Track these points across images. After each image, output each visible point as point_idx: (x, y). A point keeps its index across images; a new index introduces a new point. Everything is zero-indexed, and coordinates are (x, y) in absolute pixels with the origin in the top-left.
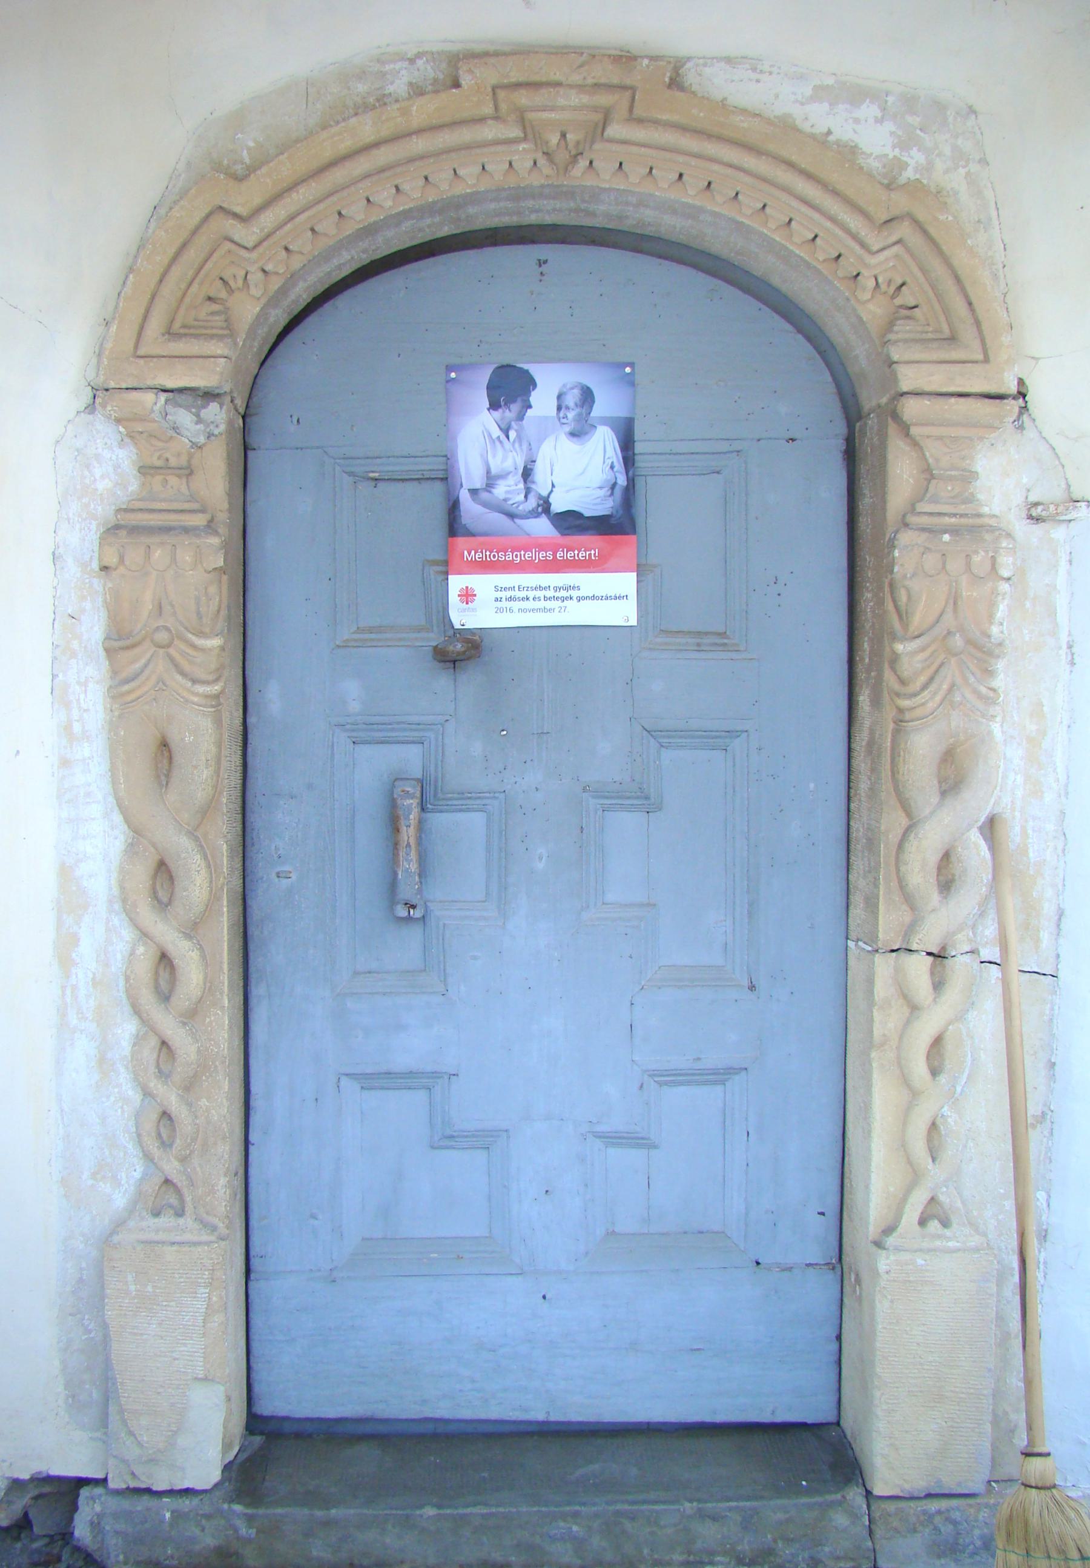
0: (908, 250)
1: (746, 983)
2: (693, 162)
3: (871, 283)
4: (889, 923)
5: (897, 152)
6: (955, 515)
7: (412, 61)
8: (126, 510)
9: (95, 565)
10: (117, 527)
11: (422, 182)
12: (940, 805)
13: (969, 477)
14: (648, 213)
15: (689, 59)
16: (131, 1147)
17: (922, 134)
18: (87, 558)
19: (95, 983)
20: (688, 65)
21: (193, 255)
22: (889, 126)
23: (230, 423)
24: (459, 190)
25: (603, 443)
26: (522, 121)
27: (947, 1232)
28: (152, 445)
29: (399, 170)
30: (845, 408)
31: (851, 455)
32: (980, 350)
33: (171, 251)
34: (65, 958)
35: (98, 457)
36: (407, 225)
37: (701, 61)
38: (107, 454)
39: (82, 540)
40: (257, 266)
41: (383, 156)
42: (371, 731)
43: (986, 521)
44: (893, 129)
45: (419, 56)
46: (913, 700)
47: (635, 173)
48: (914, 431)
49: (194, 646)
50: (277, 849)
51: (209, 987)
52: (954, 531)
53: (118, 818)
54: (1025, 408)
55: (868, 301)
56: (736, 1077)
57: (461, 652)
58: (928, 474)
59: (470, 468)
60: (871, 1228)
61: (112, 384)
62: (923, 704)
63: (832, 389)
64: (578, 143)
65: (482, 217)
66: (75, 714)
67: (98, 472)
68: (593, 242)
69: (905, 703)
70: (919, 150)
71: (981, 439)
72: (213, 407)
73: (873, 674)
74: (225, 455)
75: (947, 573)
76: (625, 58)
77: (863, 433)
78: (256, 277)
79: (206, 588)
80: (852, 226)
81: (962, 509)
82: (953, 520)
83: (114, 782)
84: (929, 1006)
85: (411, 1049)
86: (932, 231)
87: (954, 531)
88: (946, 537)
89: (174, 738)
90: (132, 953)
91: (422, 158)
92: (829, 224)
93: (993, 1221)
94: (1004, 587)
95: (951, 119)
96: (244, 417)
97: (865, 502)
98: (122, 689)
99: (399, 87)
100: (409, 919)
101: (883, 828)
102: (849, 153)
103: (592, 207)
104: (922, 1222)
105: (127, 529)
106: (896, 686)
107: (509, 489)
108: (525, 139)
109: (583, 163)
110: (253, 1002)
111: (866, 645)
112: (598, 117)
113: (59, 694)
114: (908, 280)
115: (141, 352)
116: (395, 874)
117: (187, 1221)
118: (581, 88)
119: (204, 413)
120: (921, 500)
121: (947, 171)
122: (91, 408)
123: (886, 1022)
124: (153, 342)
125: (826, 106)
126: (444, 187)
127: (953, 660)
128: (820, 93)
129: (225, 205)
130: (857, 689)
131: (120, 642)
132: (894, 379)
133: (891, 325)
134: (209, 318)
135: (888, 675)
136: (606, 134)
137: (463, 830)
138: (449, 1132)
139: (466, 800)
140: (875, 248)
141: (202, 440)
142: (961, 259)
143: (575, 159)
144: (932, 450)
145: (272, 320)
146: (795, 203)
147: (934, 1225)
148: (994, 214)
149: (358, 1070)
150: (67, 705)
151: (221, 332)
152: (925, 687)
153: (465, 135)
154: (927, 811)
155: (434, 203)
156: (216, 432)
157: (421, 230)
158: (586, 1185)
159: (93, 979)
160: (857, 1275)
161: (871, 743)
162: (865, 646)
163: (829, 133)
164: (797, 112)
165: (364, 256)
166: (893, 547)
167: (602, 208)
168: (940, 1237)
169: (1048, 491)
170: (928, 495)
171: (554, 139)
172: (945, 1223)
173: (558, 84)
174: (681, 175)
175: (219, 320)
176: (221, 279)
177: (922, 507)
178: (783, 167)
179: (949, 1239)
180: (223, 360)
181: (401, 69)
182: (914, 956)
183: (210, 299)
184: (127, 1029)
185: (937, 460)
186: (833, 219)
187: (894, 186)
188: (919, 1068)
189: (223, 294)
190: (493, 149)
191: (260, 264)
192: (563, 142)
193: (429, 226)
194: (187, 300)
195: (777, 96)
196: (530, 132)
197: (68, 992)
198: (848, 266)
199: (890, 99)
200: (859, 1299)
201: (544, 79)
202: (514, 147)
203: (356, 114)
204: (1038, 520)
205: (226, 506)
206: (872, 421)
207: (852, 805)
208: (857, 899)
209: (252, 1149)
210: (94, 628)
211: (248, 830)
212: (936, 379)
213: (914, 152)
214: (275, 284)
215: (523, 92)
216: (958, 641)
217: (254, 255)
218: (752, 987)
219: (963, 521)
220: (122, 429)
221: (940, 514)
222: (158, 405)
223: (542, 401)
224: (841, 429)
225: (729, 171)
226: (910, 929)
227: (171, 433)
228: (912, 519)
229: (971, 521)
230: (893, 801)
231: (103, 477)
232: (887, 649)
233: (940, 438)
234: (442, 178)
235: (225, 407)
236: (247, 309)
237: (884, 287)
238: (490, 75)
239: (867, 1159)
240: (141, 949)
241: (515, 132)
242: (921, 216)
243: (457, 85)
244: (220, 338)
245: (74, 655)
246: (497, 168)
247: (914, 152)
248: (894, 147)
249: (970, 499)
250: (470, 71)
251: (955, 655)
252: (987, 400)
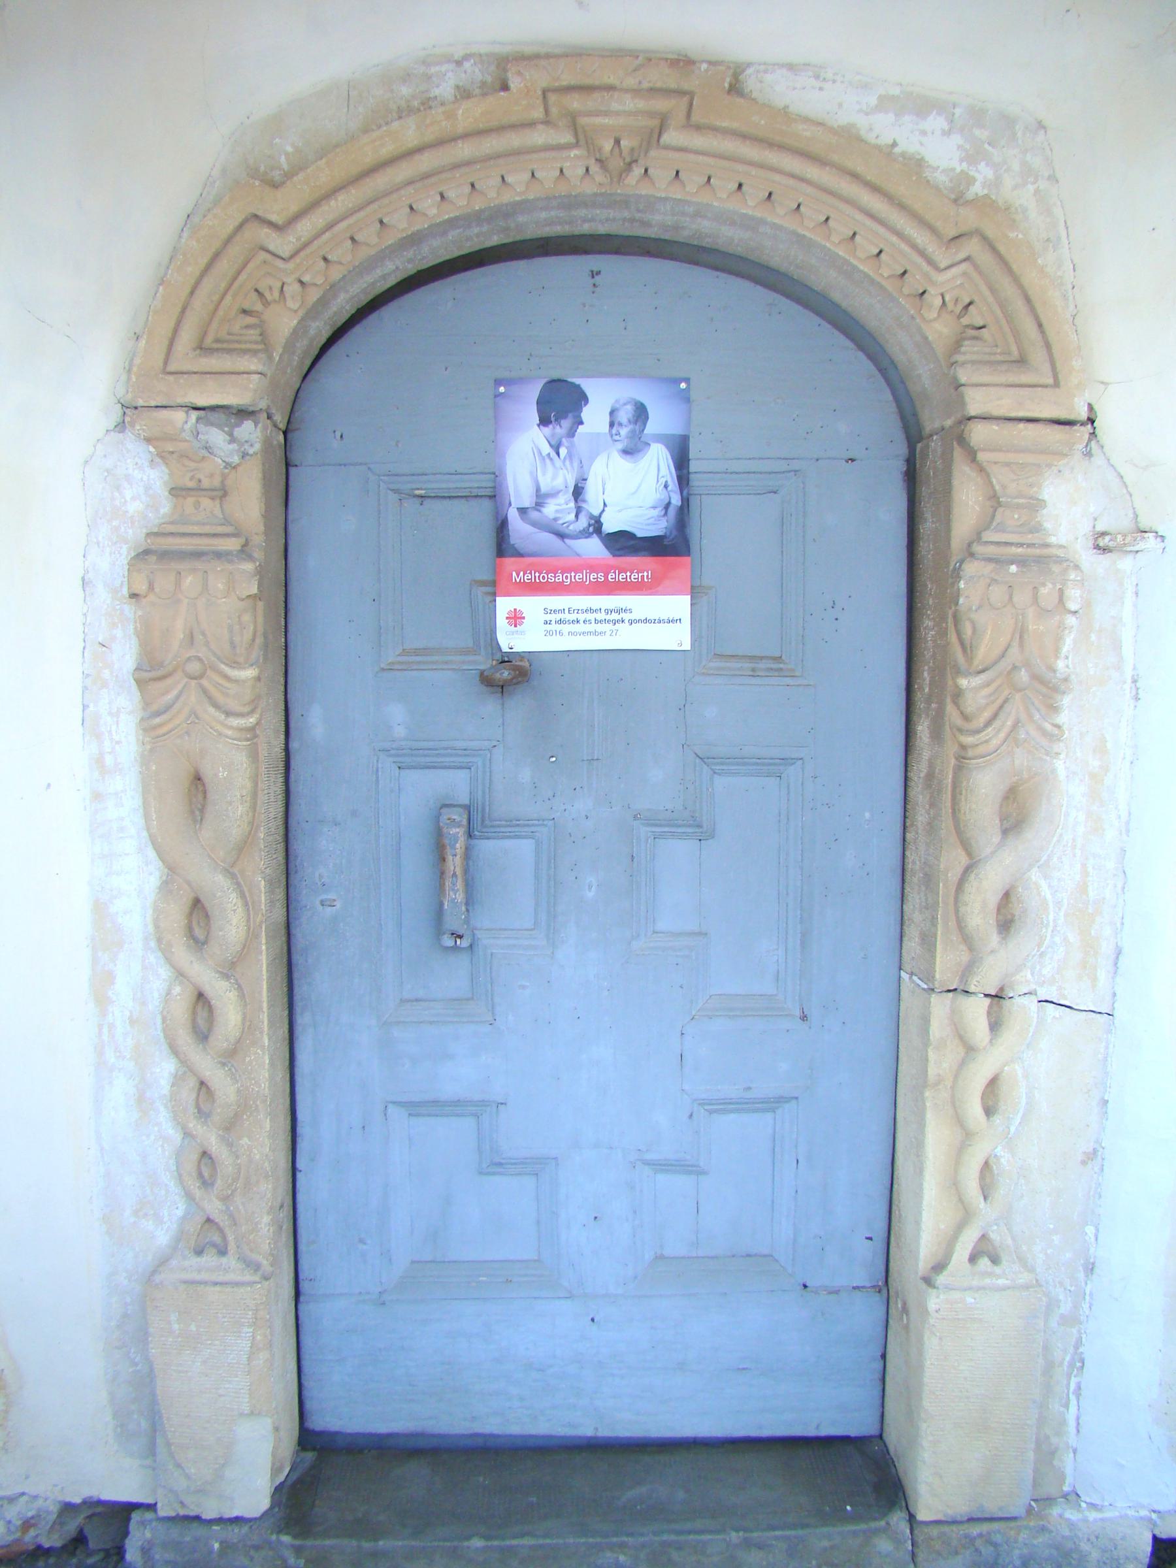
0: (976, 267)
1: (798, 1013)
2: (754, 171)
3: (939, 301)
4: (947, 962)
5: (964, 165)
6: (1021, 545)
7: (459, 63)
8: (156, 534)
9: (125, 591)
10: (147, 552)
11: (468, 189)
12: (1000, 845)
13: (1036, 505)
14: (706, 223)
15: (749, 65)
16: (173, 1185)
17: (990, 149)
18: (118, 583)
19: (132, 1021)
20: (749, 71)
21: (225, 266)
22: (957, 139)
23: (267, 443)
24: (507, 197)
25: (657, 462)
26: (574, 127)
27: (997, 1270)
28: (184, 465)
29: (444, 176)
30: (906, 428)
31: (911, 477)
32: (1050, 374)
33: (204, 261)
34: (101, 998)
35: (128, 478)
36: (453, 234)
37: (762, 67)
38: (137, 474)
39: (112, 563)
40: (294, 276)
41: (426, 162)
42: (415, 757)
43: (1054, 551)
44: (961, 142)
45: (467, 57)
46: (977, 737)
47: (693, 181)
48: (981, 456)
49: (227, 677)
50: (321, 876)
51: (248, 1027)
52: (1022, 562)
53: (151, 854)
54: (1093, 434)
55: (935, 319)
56: (787, 1106)
57: (510, 676)
58: (994, 500)
59: (519, 485)
60: (921, 1265)
61: (141, 403)
62: (986, 742)
63: (893, 408)
64: (632, 149)
65: (532, 226)
66: (107, 745)
67: (128, 494)
68: (648, 254)
69: (968, 740)
70: (987, 165)
71: (1049, 466)
72: (248, 425)
73: (933, 705)
74: (260, 475)
75: (1014, 606)
76: (683, 62)
77: (925, 456)
78: (293, 288)
79: (239, 617)
80: (919, 241)
81: (1029, 538)
82: (1020, 550)
83: (147, 816)
84: (984, 1048)
86: (1002, 249)
87: (1022, 562)
88: (1013, 568)
89: (207, 772)
90: (168, 993)
91: (468, 163)
92: (894, 239)
93: (1041, 1255)
94: (1071, 620)
95: (1019, 135)
96: (285, 433)
97: (927, 527)
98: (154, 721)
99: (445, 89)
100: (455, 948)
101: (942, 866)
102: (915, 166)
103: (647, 217)
104: (973, 1259)
105: (158, 554)
106: (959, 722)
107: (559, 508)
108: (577, 145)
109: (638, 171)
110: (298, 1030)
111: (926, 674)
112: (655, 123)
113: (91, 725)
114: (976, 299)
115: (172, 367)
116: (441, 904)
117: (230, 1261)
118: (636, 92)
119: (237, 432)
120: (987, 528)
121: (1015, 187)
122: (121, 427)
123: (940, 1063)
124: (184, 356)
125: (891, 117)
126: (492, 195)
127: (1018, 696)
128: (886, 103)
129: (260, 213)
130: (915, 718)
131: (151, 673)
132: (962, 403)
133: (957, 345)
134: (244, 332)
135: (950, 708)
136: (662, 141)
137: (511, 858)
138: (497, 1160)
139: (515, 827)
140: (942, 266)
141: (236, 459)
142: (1030, 278)
143: (629, 166)
144: (1000, 477)
145: (312, 332)
146: (859, 217)
147: (984, 1262)
148: (1063, 234)
149: (404, 1098)
150: (98, 736)
151: (255, 347)
152: (988, 724)
153: (514, 140)
154: (988, 850)
155: (481, 211)
156: (251, 451)
157: (468, 239)
158: (635, 1212)
159: (130, 1018)
160: (904, 1304)
161: (930, 776)
162: (925, 676)
163: (895, 144)
164: (862, 122)
165: (410, 266)
166: (959, 578)
167: (657, 218)
168: (990, 1274)
169: (1115, 521)
170: (994, 524)
171: (608, 146)
172: (995, 1260)
173: (610, 88)
174: (740, 185)
175: (253, 334)
176: (256, 290)
177: (989, 536)
178: (848, 178)
179: (999, 1277)
180: (256, 377)
181: (447, 71)
182: (972, 999)
183: (244, 312)
184: (165, 1068)
185: (1004, 487)
186: (899, 234)
187: (961, 201)
188: (975, 1109)
189: (259, 307)
190: (543, 155)
191: (296, 275)
192: (617, 150)
193: (478, 236)
194: (221, 313)
195: (840, 105)
196: (582, 137)
197: (105, 1030)
198: (914, 283)
199: (958, 111)
200: (907, 1327)
201: (597, 83)
202: (565, 154)
203: (400, 118)
204: (1105, 550)
205: (262, 528)
206: (935, 444)
207: (908, 835)
208: (912, 932)
209: (299, 1175)
210: (125, 656)
211: (291, 858)
212: (1004, 403)
213: (982, 166)
214: (314, 295)
215: (576, 96)
216: (1023, 676)
217: (291, 265)
218: (804, 1018)
219: (1030, 551)
220: (152, 449)
221: (1007, 544)
222: (189, 424)
223: (595, 417)
224: (902, 450)
225: (791, 182)
226: (968, 970)
227: (204, 453)
228: (977, 549)
229: (1037, 552)
230: (953, 839)
231: (134, 499)
232: (950, 682)
233: (1008, 464)
234: (489, 184)
235: (260, 425)
236: (283, 322)
237: (950, 306)
238: (541, 78)
239: (919, 1195)
240: (177, 989)
241: (567, 138)
242: (990, 233)
243: (505, 87)
244: (255, 352)
245: (105, 685)
246: (548, 175)
247: (982, 166)
248: (961, 161)
249: (1037, 529)
250: (519, 73)
251: (1020, 690)
252: (1056, 426)
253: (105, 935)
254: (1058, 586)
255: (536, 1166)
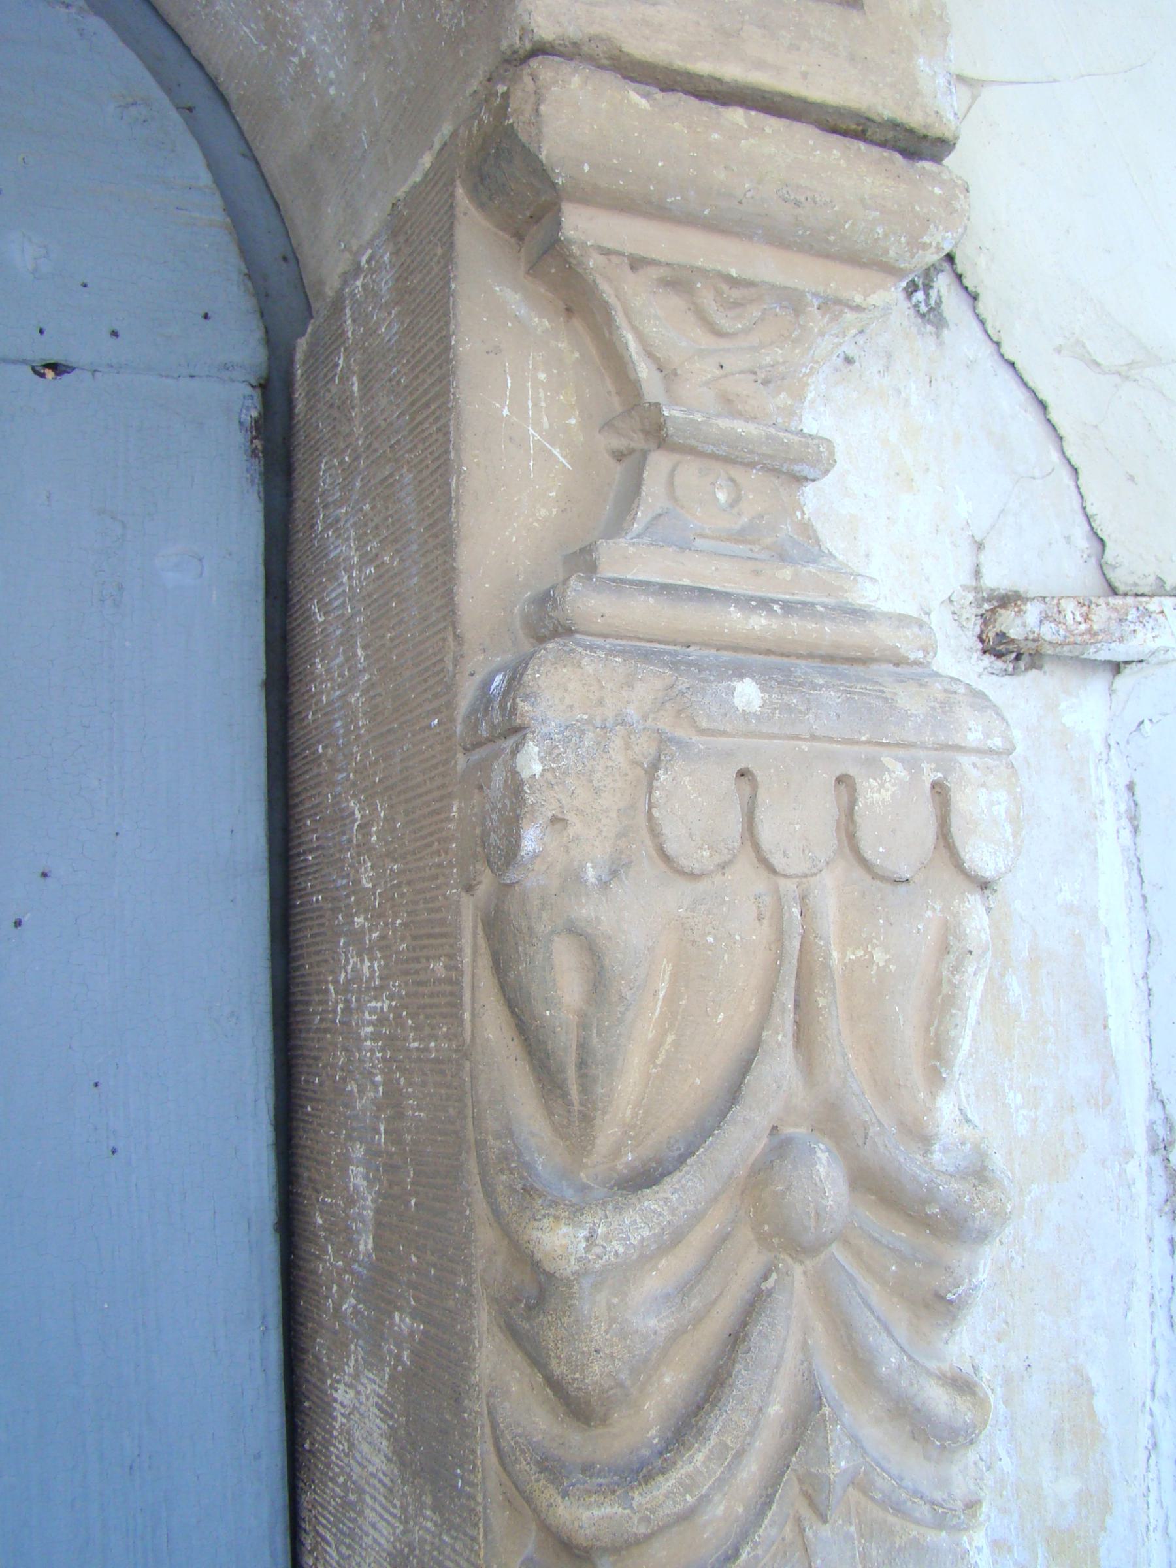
13: (792, 465)
30: (256, 278)
31: (278, 448)
43: (886, 636)
46: (638, 1498)
48: (581, 225)
52: (774, 662)
62: (687, 1516)
71: (833, 305)
73: (402, 1322)
81: (782, 581)
82: (759, 623)
87: (774, 662)
88: (747, 694)
97: (337, 602)
106: (534, 1418)
111: (357, 1177)
120: (618, 524)
127: (798, 1274)
130: (320, 1346)
135: (492, 1359)
144: (651, 323)
152: (685, 1427)
166: (516, 731)
169: (1041, 560)
170: (643, 515)
177: (627, 557)
216: (825, 1175)
221: (703, 594)
224: (245, 349)
228: (585, 603)
232: (486, 1236)
233: (679, 281)
249: (805, 547)
251: (800, 1249)
254: (930, 775)
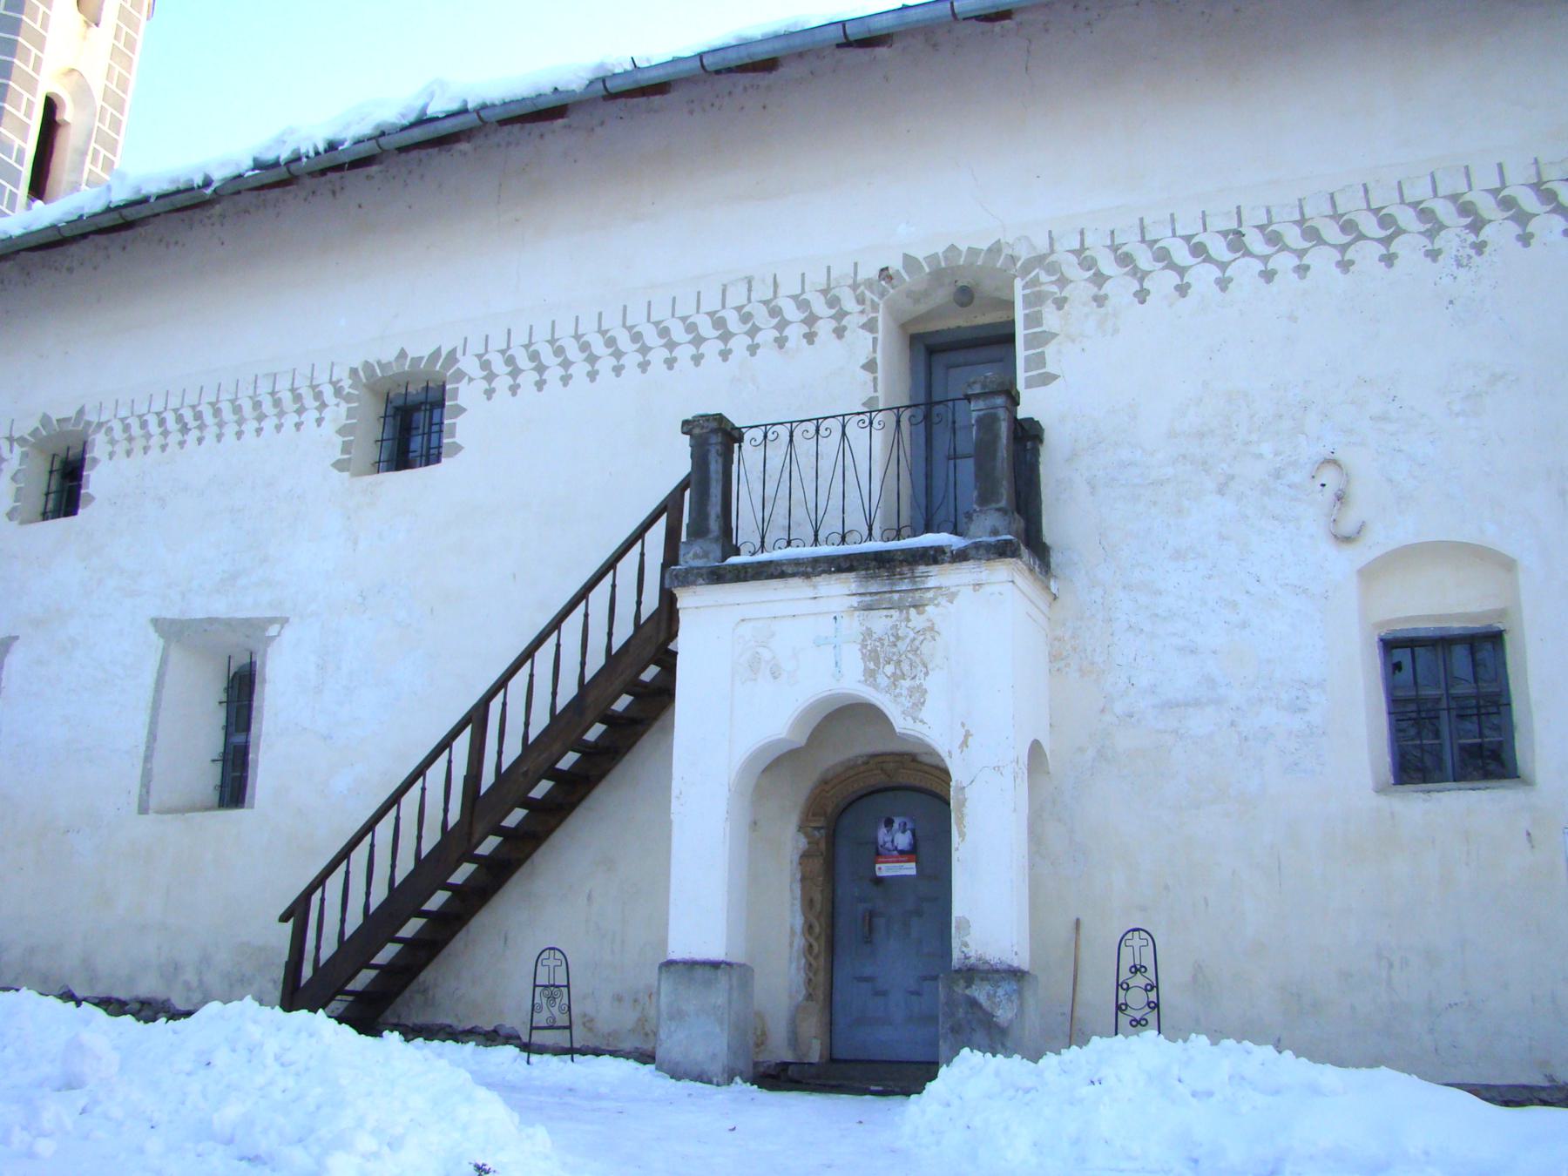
25: (908, 833)
34: (791, 945)
39: (796, 858)
57: (880, 881)
59: (881, 842)
76: (902, 754)
85: (868, 971)
98: (803, 889)
105: (805, 856)
107: (889, 845)
131: (803, 879)
137: (880, 922)
184: (803, 961)
210: (799, 876)
223: (896, 825)
236: (829, 810)
253: (793, 933)
255: (884, 993)
